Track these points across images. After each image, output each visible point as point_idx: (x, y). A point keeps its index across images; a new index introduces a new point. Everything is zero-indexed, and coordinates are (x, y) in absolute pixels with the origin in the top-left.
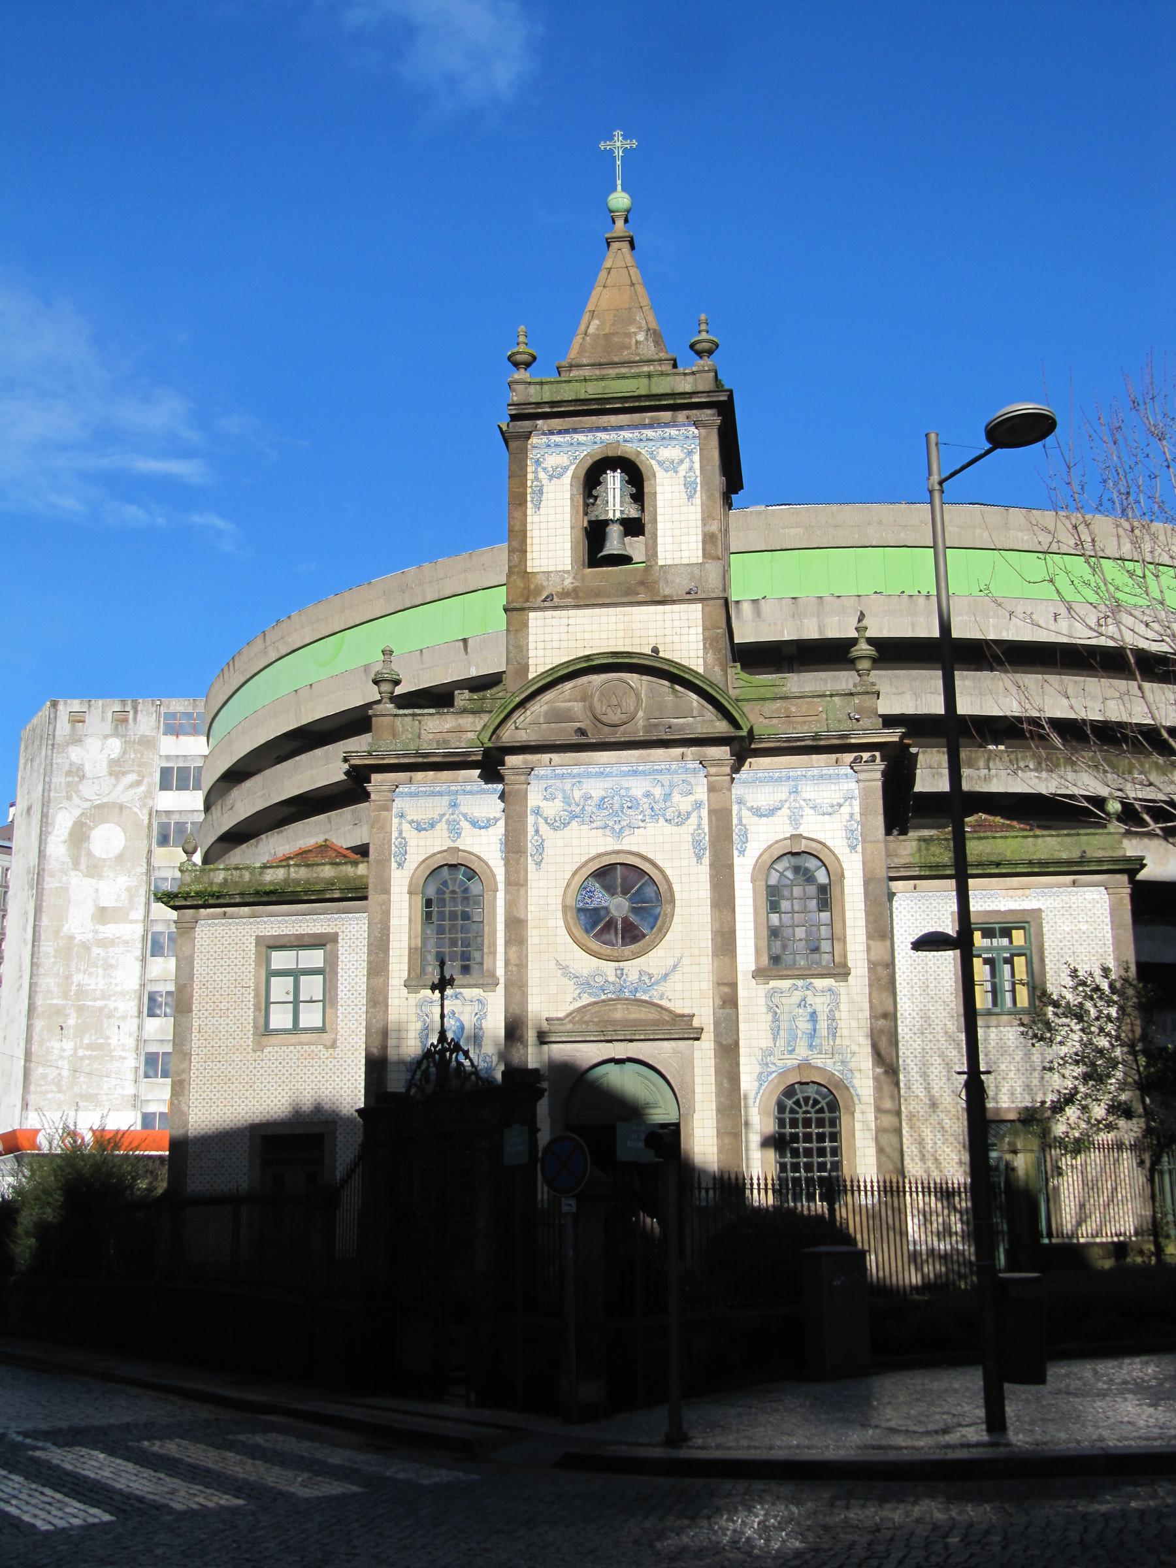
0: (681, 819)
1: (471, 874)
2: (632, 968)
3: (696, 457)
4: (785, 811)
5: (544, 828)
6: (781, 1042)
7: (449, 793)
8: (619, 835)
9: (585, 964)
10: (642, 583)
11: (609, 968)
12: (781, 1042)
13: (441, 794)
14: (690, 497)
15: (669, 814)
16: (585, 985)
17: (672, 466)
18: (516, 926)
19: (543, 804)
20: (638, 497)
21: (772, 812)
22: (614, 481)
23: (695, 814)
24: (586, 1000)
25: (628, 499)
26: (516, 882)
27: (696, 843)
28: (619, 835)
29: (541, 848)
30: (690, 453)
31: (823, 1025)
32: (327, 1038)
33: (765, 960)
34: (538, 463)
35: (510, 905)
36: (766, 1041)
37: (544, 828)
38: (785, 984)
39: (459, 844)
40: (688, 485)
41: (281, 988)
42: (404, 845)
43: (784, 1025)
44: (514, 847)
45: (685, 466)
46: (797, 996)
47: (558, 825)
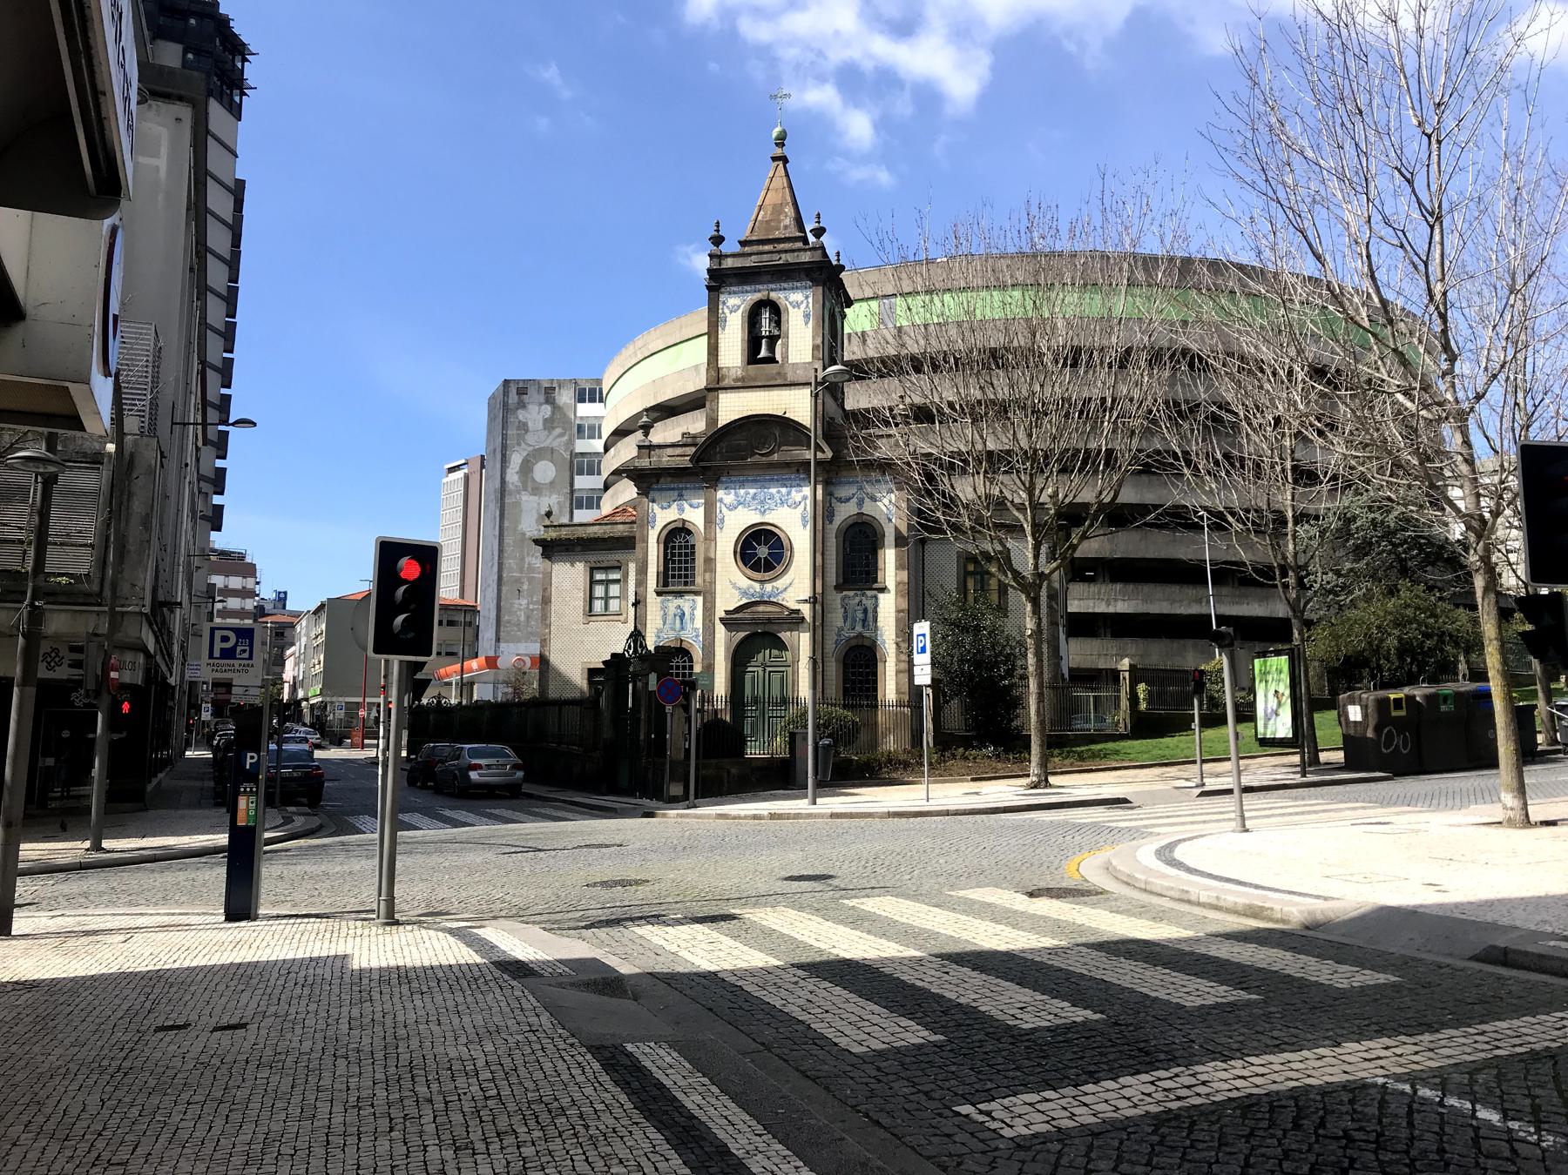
0: (796, 505)
1: (689, 532)
2: (768, 587)
3: (810, 300)
4: (855, 500)
5: (724, 509)
6: (848, 623)
7: (678, 489)
8: (763, 513)
9: (744, 582)
10: (779, 373)
11: (757, 586)
12: (848, 623)
13: (673, 489)
14: (806, 323)
15: (790, 502)
16: (744, 593)
17: (797, 305)
18: (710, 562)
19: (724, 497)
20: (778, 324)
21: (848, 500)
22: (766, 315)
23: (803, 504)
24: (744, 601)
25: (773, 324)
26: (710, 538)
27: (804, 518)
28: (763, 513)
29: (722, 520)
30: (807, 297)
31: (870, 615)
32: (621, 618)
33: (841, 581)
34: (724, 303)
35: (707, 550)
36: (840, 623)
37: (724, 509)
38: (851, 593)
39: (684, 516)
40: (807, 316)
41: (599, 591)
42: (654, 516)
43: (850, 615)
44: (710, 519)
45: (804, 305)
46: (857, 599)
47: (732, 508)
